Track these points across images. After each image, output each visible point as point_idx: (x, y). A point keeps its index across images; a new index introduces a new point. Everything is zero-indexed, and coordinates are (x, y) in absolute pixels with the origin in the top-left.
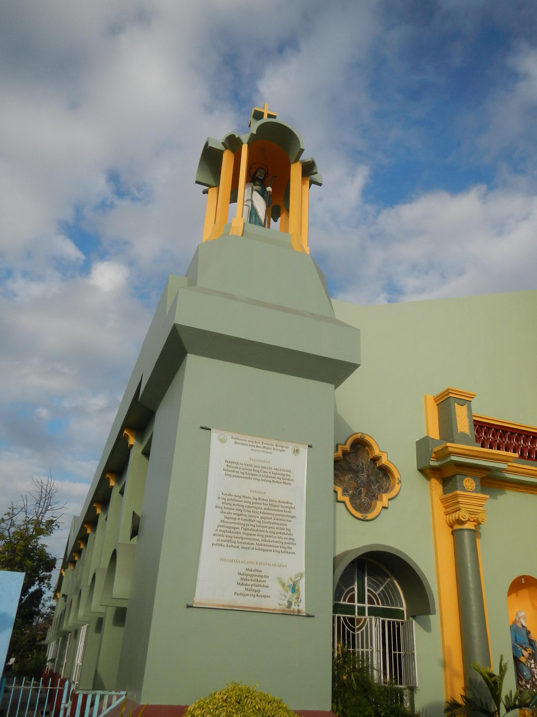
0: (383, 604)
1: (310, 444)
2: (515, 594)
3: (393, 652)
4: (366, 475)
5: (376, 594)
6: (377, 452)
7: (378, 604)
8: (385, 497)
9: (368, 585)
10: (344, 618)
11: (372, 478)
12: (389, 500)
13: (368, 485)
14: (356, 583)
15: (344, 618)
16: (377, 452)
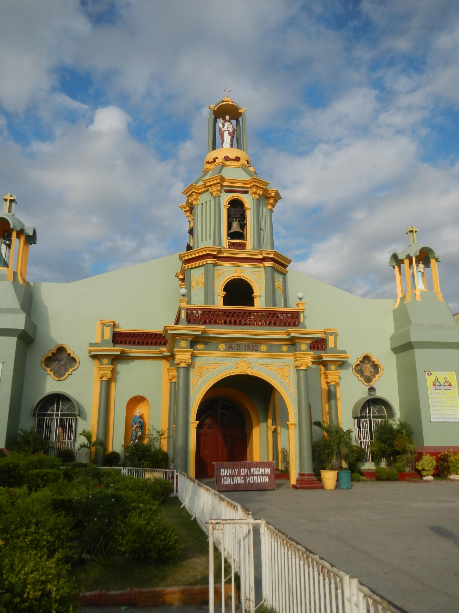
0: (67, 412)
1: (3, 362)
2: (143, 403)
3: (70, 429)
4: (64, 362)
5: (65, 408)
6: (69, 352)
7: (65, 412)
8: (71, 370)
9: (61, 405)
10: (49, 418)
11: (67, 362)
12: (72, 371)
13: (65, 365)
14: (55, 405)
15: (49, 418)
16: (69, 352)
